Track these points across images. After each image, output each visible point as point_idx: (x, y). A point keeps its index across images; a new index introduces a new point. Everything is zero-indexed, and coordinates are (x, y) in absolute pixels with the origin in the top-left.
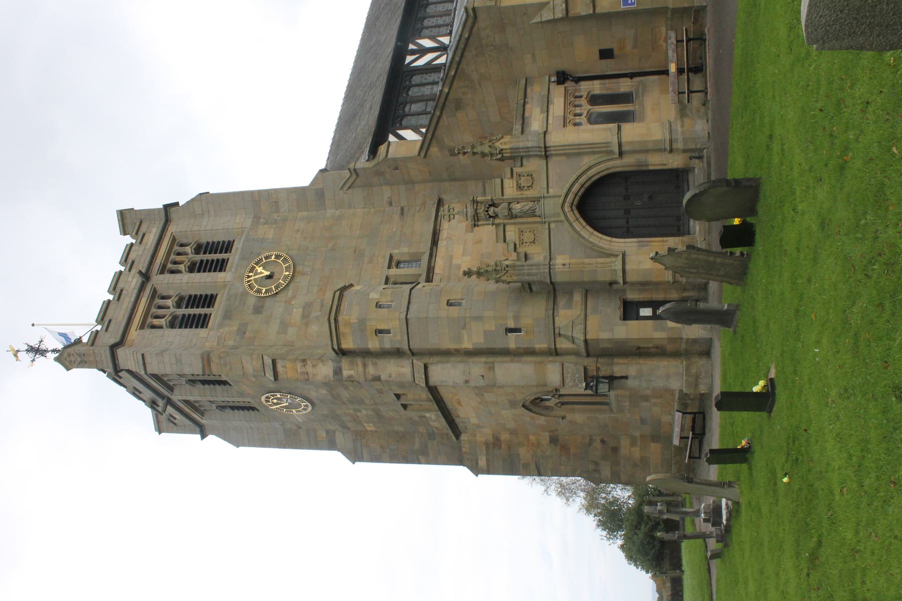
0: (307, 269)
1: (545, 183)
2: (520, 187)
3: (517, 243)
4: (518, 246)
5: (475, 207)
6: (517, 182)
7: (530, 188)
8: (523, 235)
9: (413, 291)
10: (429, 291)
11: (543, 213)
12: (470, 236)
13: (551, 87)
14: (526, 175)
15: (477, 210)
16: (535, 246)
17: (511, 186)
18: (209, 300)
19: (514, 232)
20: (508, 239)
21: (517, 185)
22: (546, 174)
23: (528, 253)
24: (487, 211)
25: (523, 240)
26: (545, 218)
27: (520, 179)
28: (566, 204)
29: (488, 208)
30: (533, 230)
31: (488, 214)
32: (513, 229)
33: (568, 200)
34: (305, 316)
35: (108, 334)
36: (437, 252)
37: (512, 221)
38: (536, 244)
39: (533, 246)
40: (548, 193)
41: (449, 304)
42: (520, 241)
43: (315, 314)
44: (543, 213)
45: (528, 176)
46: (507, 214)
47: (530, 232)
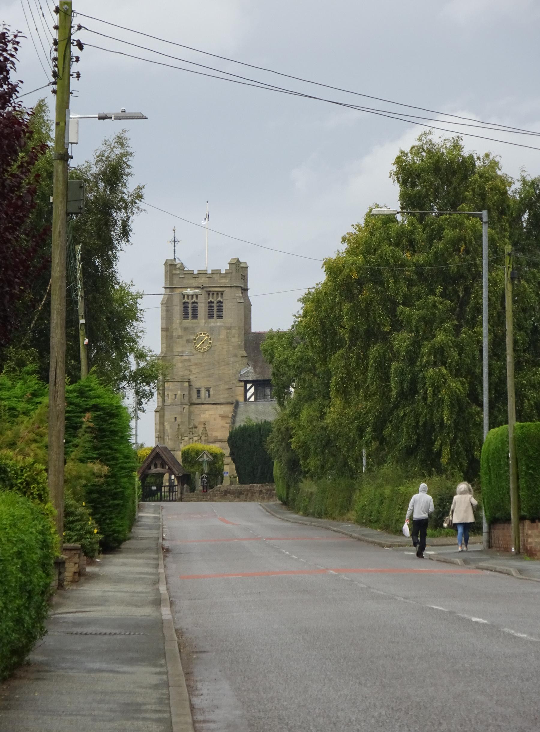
0: (205, 356)
12: (218, 416)
18: (195, 317)
34: (185, 360)
35: (178, 279)
41: (176, 418)
43: (186, 364)
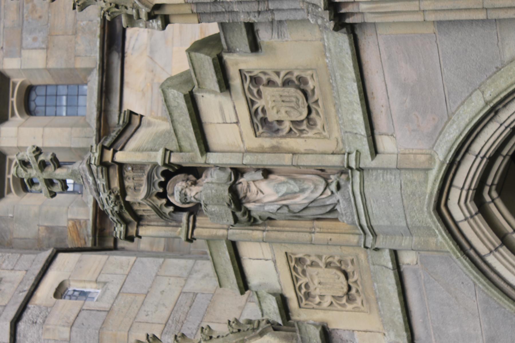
1: (359, 117)
2: (264, 121)
3: (290, 294)
4: (293, 304)
5: (115, 184)
6: (251, 103)
7: (304, 126)
8: (304, 272)
9: (22, 326)
10: (66, 335)
11: (364, 223)
13: (175, 142)
14: (279, 81)
15: (123, 191)
16: (356, 309)
17: (231, 117)
19: (271, 264)
20: (253, 280)
21: (253, 114)
22: (354, 87)
23: (332, 326)
24: (162, 195)
25: (307, 286)
26: (375, 235)
27: (259, 92)
28: (455, 194)
29: (163, 185)
30: (340, 262)
31: (169, 204)
32: (269, 256)
33: (459, 180)
36: (126, 71)
37: (257, 234)
38: (359, 300)
39: (349, 307)
40: (375, 151)
42: (297, 289)
44: (364, 223)
45: (286, 83)
46: (232, 222)
47: (328, 265)
